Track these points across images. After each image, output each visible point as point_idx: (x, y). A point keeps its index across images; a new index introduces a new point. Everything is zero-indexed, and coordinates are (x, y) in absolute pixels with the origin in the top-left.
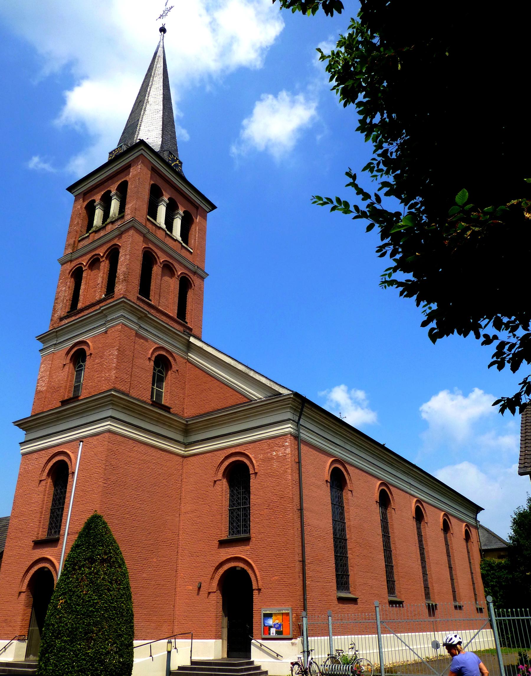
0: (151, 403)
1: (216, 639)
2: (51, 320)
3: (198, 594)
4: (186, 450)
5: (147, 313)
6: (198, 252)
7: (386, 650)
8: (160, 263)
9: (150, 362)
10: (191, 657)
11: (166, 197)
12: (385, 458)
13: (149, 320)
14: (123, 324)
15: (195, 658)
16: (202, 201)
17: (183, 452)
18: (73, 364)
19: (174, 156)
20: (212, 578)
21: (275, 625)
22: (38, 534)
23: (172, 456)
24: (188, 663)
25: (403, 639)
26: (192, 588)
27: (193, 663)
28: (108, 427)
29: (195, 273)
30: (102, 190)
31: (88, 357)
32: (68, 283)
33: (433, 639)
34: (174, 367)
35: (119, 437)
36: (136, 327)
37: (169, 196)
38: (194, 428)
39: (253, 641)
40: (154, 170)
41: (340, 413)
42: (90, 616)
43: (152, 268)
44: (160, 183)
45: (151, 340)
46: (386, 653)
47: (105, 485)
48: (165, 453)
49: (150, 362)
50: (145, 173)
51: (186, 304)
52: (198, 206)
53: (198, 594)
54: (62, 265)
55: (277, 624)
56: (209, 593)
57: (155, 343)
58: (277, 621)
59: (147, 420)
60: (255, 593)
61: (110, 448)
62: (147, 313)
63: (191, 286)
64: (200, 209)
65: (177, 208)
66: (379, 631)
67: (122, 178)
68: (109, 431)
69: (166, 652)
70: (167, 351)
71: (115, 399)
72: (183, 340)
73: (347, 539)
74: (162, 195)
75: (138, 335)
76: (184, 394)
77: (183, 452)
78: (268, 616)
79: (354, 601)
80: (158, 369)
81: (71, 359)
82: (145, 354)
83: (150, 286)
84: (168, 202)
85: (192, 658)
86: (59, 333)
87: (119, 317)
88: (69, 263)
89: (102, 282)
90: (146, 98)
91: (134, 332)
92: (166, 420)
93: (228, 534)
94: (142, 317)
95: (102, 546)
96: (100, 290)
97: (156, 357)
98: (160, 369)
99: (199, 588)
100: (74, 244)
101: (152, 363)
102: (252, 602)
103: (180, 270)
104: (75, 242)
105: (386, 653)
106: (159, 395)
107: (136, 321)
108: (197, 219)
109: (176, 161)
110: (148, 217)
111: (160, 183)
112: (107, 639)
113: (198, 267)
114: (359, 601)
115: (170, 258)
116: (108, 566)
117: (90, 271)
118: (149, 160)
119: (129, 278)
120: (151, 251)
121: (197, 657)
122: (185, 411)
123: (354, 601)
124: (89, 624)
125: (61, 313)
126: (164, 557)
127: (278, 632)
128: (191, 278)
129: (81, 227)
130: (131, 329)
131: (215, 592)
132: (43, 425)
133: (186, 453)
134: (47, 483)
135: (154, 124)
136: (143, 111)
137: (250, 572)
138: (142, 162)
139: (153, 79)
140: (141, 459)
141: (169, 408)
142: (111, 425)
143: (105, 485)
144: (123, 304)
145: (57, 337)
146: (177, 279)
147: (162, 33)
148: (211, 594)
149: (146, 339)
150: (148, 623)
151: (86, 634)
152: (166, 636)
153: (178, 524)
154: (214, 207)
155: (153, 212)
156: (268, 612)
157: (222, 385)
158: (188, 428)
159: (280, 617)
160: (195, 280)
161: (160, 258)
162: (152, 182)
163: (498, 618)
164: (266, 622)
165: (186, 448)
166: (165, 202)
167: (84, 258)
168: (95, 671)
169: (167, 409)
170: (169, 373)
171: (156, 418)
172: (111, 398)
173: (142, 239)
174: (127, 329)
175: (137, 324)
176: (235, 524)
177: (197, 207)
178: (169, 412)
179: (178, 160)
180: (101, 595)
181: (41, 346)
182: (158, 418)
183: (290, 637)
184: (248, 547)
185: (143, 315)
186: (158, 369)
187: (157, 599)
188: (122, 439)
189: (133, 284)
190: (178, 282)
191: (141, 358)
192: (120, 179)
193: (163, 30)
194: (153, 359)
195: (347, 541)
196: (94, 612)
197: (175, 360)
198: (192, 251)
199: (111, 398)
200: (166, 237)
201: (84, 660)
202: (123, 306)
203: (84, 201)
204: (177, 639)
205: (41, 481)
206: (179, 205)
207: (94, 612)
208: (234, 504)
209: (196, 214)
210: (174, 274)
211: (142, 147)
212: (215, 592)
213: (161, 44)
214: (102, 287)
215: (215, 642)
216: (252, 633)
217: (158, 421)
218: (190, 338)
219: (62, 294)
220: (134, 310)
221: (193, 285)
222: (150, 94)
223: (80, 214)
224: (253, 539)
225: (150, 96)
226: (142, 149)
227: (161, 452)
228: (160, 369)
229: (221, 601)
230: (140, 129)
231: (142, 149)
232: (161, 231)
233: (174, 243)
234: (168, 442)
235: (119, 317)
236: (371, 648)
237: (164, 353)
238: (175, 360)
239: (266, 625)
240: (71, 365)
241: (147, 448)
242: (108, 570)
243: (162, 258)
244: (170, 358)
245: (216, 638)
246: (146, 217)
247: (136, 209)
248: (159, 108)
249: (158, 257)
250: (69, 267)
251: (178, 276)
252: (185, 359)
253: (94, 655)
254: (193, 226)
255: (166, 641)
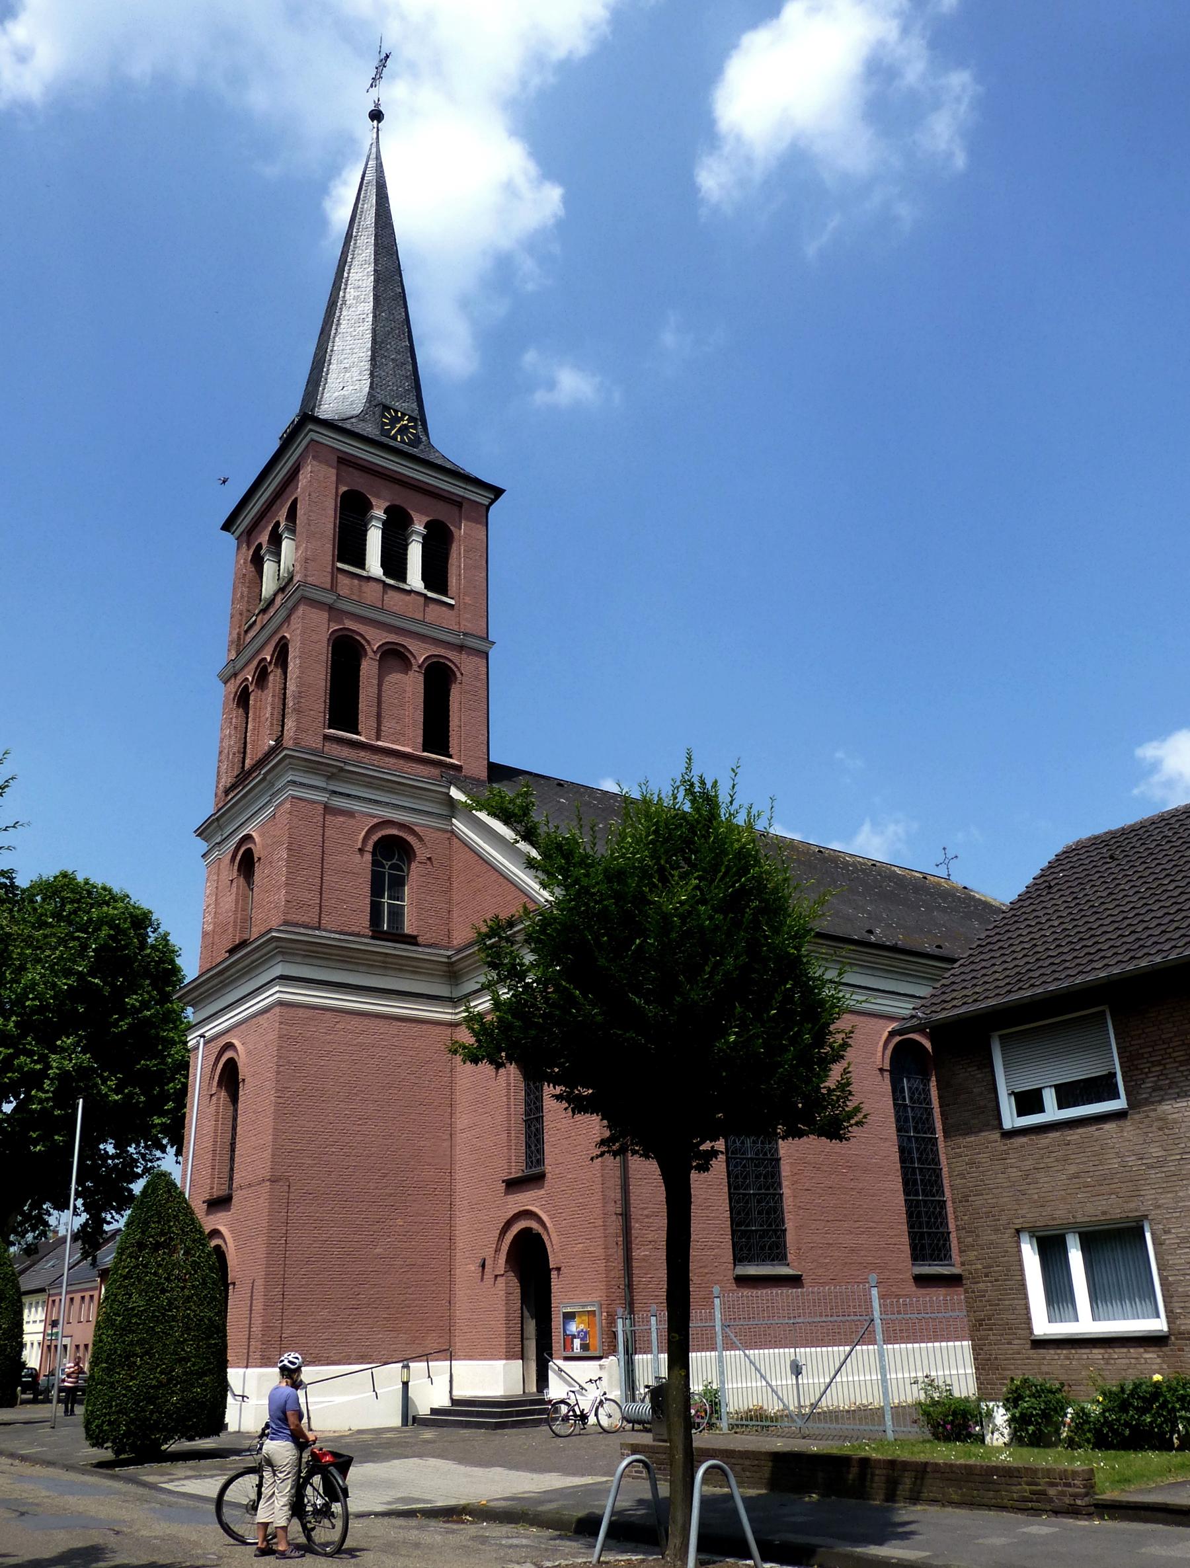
0: (370, 934)
1: (507, 1359)
2: (216, 795)
3: (482, 1279)
4: (457, 1011)
5: (342, 765)
6: (467, 600)
7: (893, 1376)
8: (374, 652)
9: (362, 856)
10: (451, 1392)
11: (379, 507)
12: (911, 970)
13: (348, 775)
14: (293, 798)
15: (458, 1393)
16: (468, 487)
17: (449, 1017)
18: (245, 877)
19: (394, 410)
20: (497, 1250)
21: (579, 1332)
22: (212, 1188)
23: (425, 1027)
24: (445, 1402)
25: (752, 1358)
26: (474, 1267)
27: (454, 1402)
28: (277, 995)
29: (461, 648)
30: (266, 527)
31: (257, 865)
32: (234, 720)
33: (793, 1357)
34: (421, 852)
35: (301, 1011)
36: (322, 797)
37: (387, 504)
38: (466, 968)
39: (551, 1363)
40: (344, 462)
41: (944, 849)
42: (134, 1332)
43: (360, 666)
44: (360, 482)
45: (362, 812)
46: (894, 1382)
47: (280, 1100)
48: (408, 1025)
49: (362, 856)
50: (322, 479)
51: (449, 716)
52: (459, 499)
53: (482, 1279)
54: (225, 683)
55: (582, 1331)
56: (496, 1276)
57: (371, 816)
58: (582, 1327)
59: (361, 969)
60: (554, 1274)
61: (285, 1033)
62: (342, 765)
63: (456, 678)
64: (465, 505)
65: (409, 521)
66: (879, 1337)
67: (291, 497)
68: (281, 1003)
69: (401, 1386)
70: (402, 826)
71: (283, 944)
72: (438, 796)
73: (780, 1159)
74: (369, 506)
75: (328, 809)
76: (449, 902)
77: (449, 1017)
78: (569, 1317)
79: (795, 1281)
80: (389, 863)
81: (239, 870)
82: (349, 842)
83: (358, 703)
84: (384, 517)
85: (455, 1393)
86: (221, 821)
87: (285, 787)
88: (232, 681)
89: (272, 714)
90: (341, 294)
91: (320, 808)
92: (400, 962)
93: (524, 1168)
94: (333, 774)
95: (159, 1222)
96: (268, 732)
97: (376, 844)
98: (394, 861)
99: (483, 1266)
100: (239, 638)
101: (368, 857)
102: (550, 1292)
103: (421, 653)
104: (239, 634)
105: (894, 1382)
106: (397, 914)
107: (323, 785)
108: (460, 529)
109: (402, 419)
110: (339, 565)
111: (360, 482)
112: (158, 1366)
113: (465, 634)
114: (806, 1280)
115: (396, 634)
116: (164, 1253)
117: (260, 692)
118: (327, 445)
119: (302, 705)
120: (350, 634)
121: (464, 1391)
122: (455, 934)
123: (795, 1281)
124: (131, 1343)
125: (227, 781)
126: (421, 1215)
127: (585, 1347)
128: (451, 661)
129: (248, 602)
130: (314, 802)
131: (502, 1275)
132: (210, 995)
133: (457, 1017)
134: (219, 1099)
135: (355, 351)
136: (334, 327)
137: (545, 1237)
138: (313, 457)
139: (355, 244)
140: (355, 1042)
141: (415, 937)
142: (281, 992)
143: (280, 1100)
144: (287, 761)
145: (221, 828)
146: (417, 674)
147: (375, 122)
148: (499, 1279)
149: (350, 814)
150: (393, 1334)
151: (127, 1358)
152: (400, 1357)
153: (448, 1153)
154: (498, 492)
155: (351, 549)
156: (569, 1310)
157: (502, 880)
158: (455, 968)
159: (585, 1318)
160: (465, 665)
161: (372, 642)
162: (343, 489)
163: (884, 1316)
164: (568, 1327)
165: (456, 1007)
166: (378, 519)
167: (246, 670)
168: (141, 1412)
169: (412, 940)
170: (413, 865)
171: (379, 962)
172: (274, 944)
173: (325, 615)
174: (304, 804)
175: (324, 790)
176: (533, 1148)
177: (457, 503)
178: (417, 944)
179: (406, 415)
180: (151, 1299)
181: (203, 846)
182: (384, 962)
183: (597, 1354)
184: (542, 1192)
185: (335, 770)
186: (389, 863)
187: (410, 1291)
188: (310, 1013)
189: (312, 712)
190: (421, 678)
191: (341, 852)
192: (288, 499)
193: (377, 115)
194: (369, 848)
195: (782, 1162)
196: (139, 1324)
197: (420, 839)
198: (452, 602)
199: (274, 944)
200: (384, 592)
201: (124, 1395)
202: (290, 764)
203: (249, 548)
204: (432, 1360)
205: (212, 1095)
206: (412, 513)
207: (139, 1324)
208: (531, 1110)
209: (457, 520)
210: (411, 665)
211: (310, 427)
212: (502, 1275)
213: (374, 150)
214: (272, 725)
215: (504, 1365)
216: (551, 1348)
217: (385, 968)
218: (449, 788)
219: (226, 744)
220: (312, 765)
221: (458, 674)
222: (349, 282)
223: (245, 575)
224: (548, 1176)
225: (349, 287)
226: (311, 430)
227: (399, 1024)
228: (394, 861)
229: (517, 1291)
230: (328, 370)
231: (311, 430)
232: (372, 584)
233: (408, 598)
234: (413, 1002)
235: (285, 787)
236: (906, 1368)
237: (395, 832)
238: (420, 839)
239: (568, 1333)
240: (242, 879)
241: (366, 1021)
242: (163, 1259)
243: (375, 639)
244: (410, 839)
245: (264, 1365)
246: (333, 565)
247: (307, 559)
248: (367, 308)
249: (368, 642)
250: (233, 686)
251: (419, 667)
252: (446, 831)
253: (138, 1389)
254: (454, 547)
255: (400, 1365)
